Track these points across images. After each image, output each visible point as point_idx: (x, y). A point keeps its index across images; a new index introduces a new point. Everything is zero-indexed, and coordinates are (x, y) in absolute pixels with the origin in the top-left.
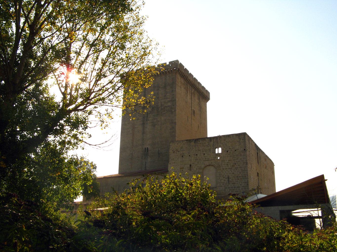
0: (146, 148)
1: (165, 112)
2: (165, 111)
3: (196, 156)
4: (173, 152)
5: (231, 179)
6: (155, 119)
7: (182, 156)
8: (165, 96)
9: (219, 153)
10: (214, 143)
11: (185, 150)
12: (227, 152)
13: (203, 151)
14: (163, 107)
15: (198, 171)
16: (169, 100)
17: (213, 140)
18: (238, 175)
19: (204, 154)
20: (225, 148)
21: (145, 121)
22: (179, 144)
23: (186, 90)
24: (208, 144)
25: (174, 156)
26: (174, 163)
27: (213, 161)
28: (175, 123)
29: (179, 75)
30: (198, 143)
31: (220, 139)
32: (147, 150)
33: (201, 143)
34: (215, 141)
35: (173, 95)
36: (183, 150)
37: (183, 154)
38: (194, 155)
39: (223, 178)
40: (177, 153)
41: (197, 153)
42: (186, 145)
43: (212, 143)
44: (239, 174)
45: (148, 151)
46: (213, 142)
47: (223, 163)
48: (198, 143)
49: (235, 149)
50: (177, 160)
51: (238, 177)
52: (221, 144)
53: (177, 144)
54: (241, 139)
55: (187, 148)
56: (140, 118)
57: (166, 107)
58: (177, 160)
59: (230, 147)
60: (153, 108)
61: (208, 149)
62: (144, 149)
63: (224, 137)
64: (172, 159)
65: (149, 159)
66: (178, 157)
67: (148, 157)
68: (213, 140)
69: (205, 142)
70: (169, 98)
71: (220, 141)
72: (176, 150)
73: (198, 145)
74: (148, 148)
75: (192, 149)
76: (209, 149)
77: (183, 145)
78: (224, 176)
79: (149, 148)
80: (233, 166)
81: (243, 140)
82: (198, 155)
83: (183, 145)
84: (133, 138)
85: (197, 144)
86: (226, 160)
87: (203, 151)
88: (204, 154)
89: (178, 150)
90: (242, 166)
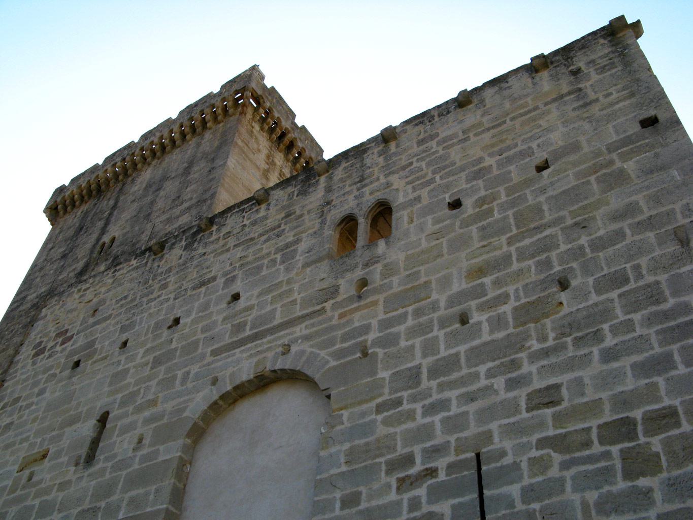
5: (514, 490)
12: (456, 205)
15: (144, 459)
18: (623, 401)
27: (299, 330)
29: (262, 129)
39: (404, 484)
41: (178, 313)
44: (630, 384)
47: (402, 318)
49: (540, 156)
51: (622, 429)
78: (409, 460)
80: (529, 313)
86: (445, 282)
90: (663, 278)
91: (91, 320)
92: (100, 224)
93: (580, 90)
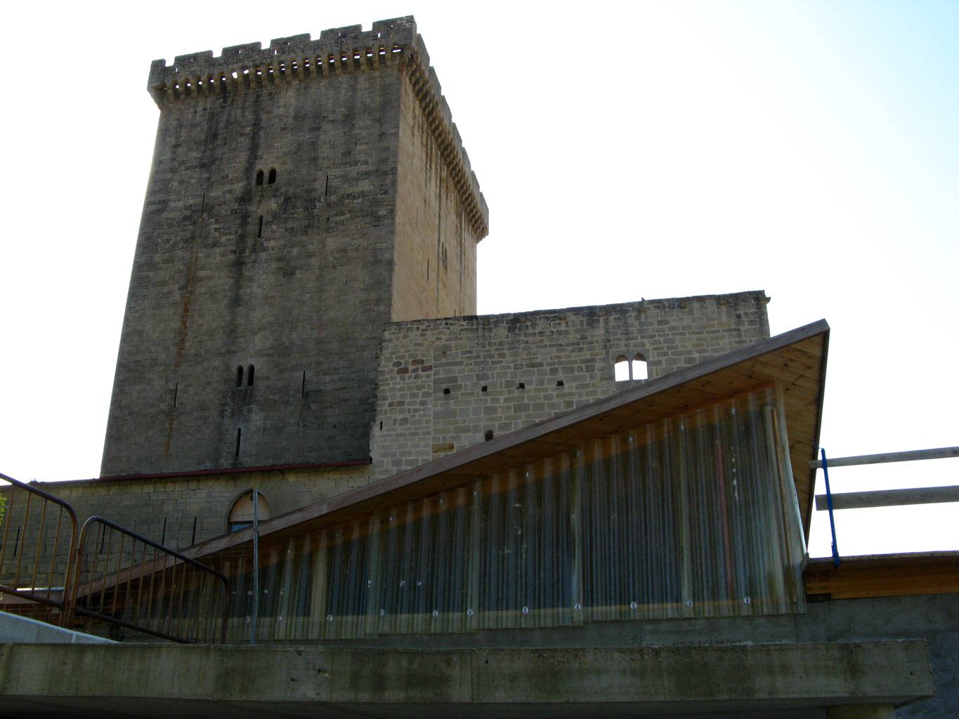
0: (246, 370)
1: (342, 218)
2: (343, 214)
3: (517, 393)
4: (399, 372)
6: (293, 246)
7: (447, 391)
8: (349, 153)
9: (636, 377)
10: (607, 331)
11: (460, 363)
13: (554, 371)
14: (333, 198)
16: (363, 168)
17: (606, 322)
19: (560, 384)
20: (664, 359)
21: (247, 253)
22: (428, 333)
23: (427, 155)
24: (579, 336)
25: (401, 389)
26: (404, 421)
28: (391, 263)
30: (530, 331)
31: (638, 318)
32: (247, 377)
33: (541, 333)
34: (612, 323)
35: (387, 149)
36: (449, 364)
37: (454, 380)
38: (508, 384)
40: (416, 377)
42: (469, 339)
43: (599, 332)
45: (251, 382)
46: (602, 332)
48: (530, 331)
50: (416, 410)
52: (646, 341)
53: (418, 333)
54: (744, 318)
55: (470, 352)
56: (223, 239)
57: (349, 196)
58: (418, 406)
59: (691, 352)
60: (287, 200)
61: (582, 362)
62: (234, 370)
63: (656, 307)
64: (391, 405)
65: (257, 418)
66: (426, 395)
67: (254, 406)
68: (606, 322)
69: (563, 328)
70: (366, 163)
71: (641, 324)
72: (415, 362)
73: (530, 339)
74: (252, 369)
75: (496, 359)
76: (587, 361)
77: (449, 339)
79: (256, 368)
81: (751, 322)
82: (526, 387)
83: (449, 339)
84: (184, 323)
85: (522, 338)
87: (554, 371)
88: (560, 384)
89: (422, 362)
91: (443, 360)
92: (244, 142)
93: (739, 330)
